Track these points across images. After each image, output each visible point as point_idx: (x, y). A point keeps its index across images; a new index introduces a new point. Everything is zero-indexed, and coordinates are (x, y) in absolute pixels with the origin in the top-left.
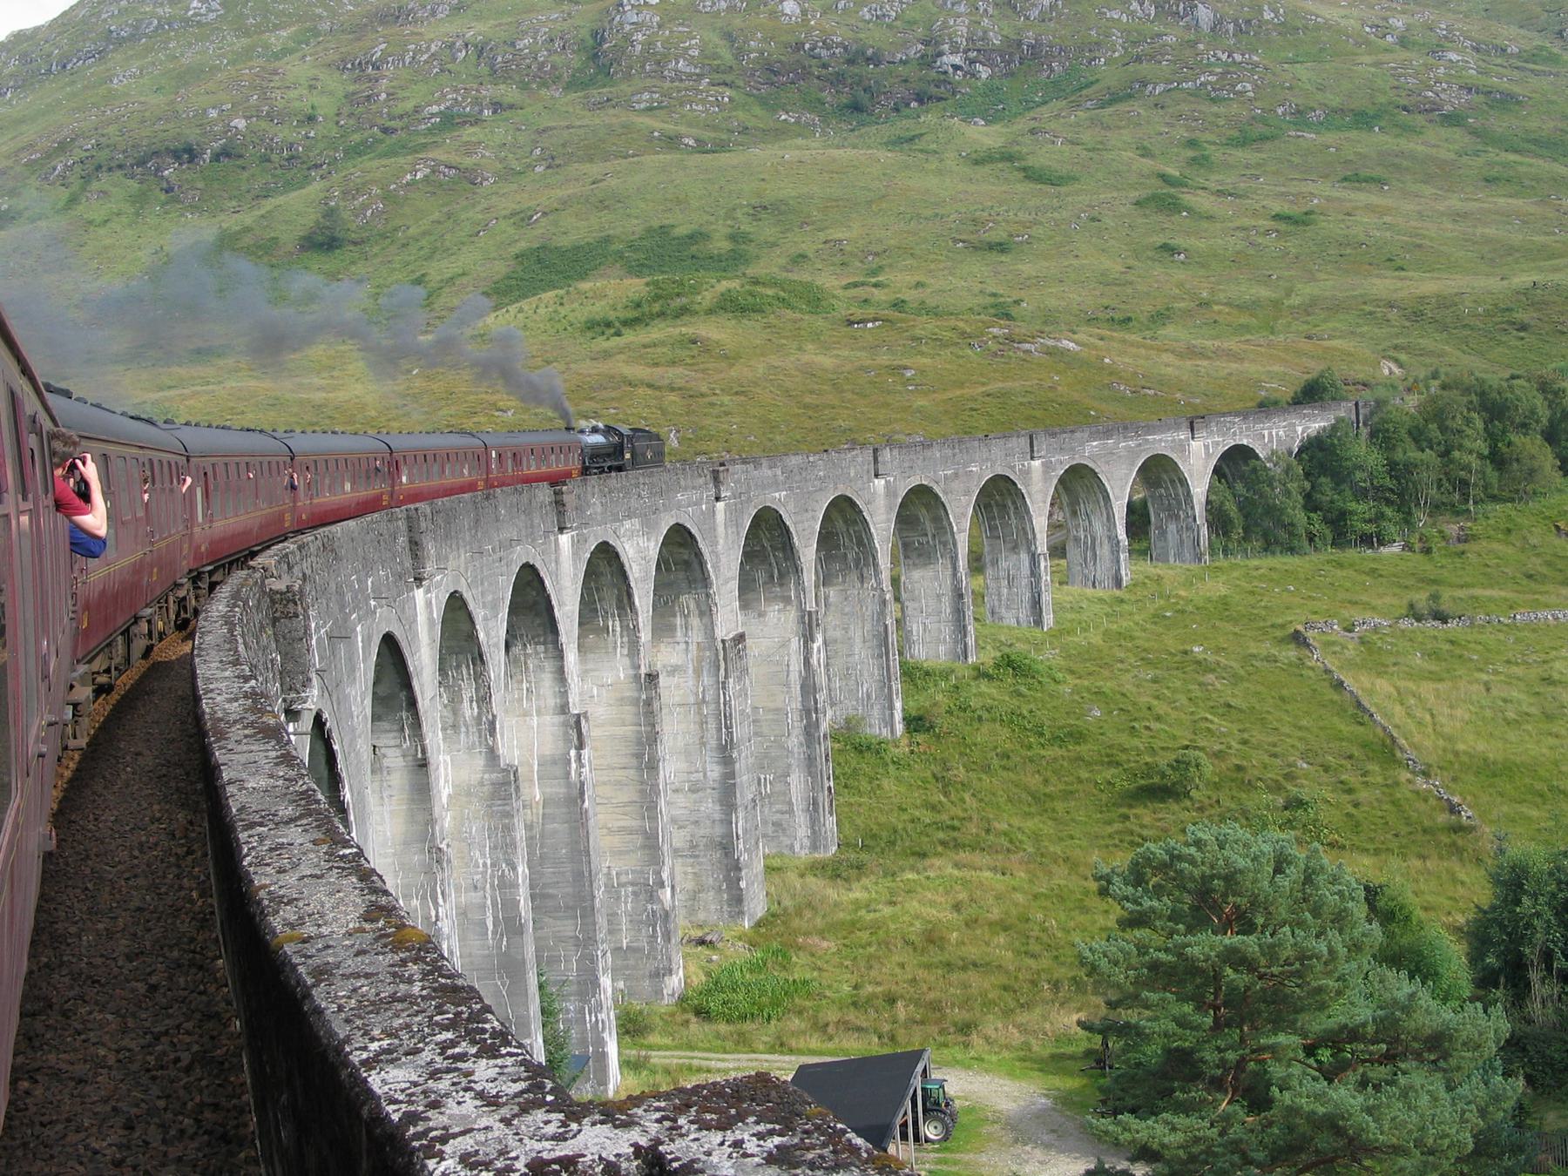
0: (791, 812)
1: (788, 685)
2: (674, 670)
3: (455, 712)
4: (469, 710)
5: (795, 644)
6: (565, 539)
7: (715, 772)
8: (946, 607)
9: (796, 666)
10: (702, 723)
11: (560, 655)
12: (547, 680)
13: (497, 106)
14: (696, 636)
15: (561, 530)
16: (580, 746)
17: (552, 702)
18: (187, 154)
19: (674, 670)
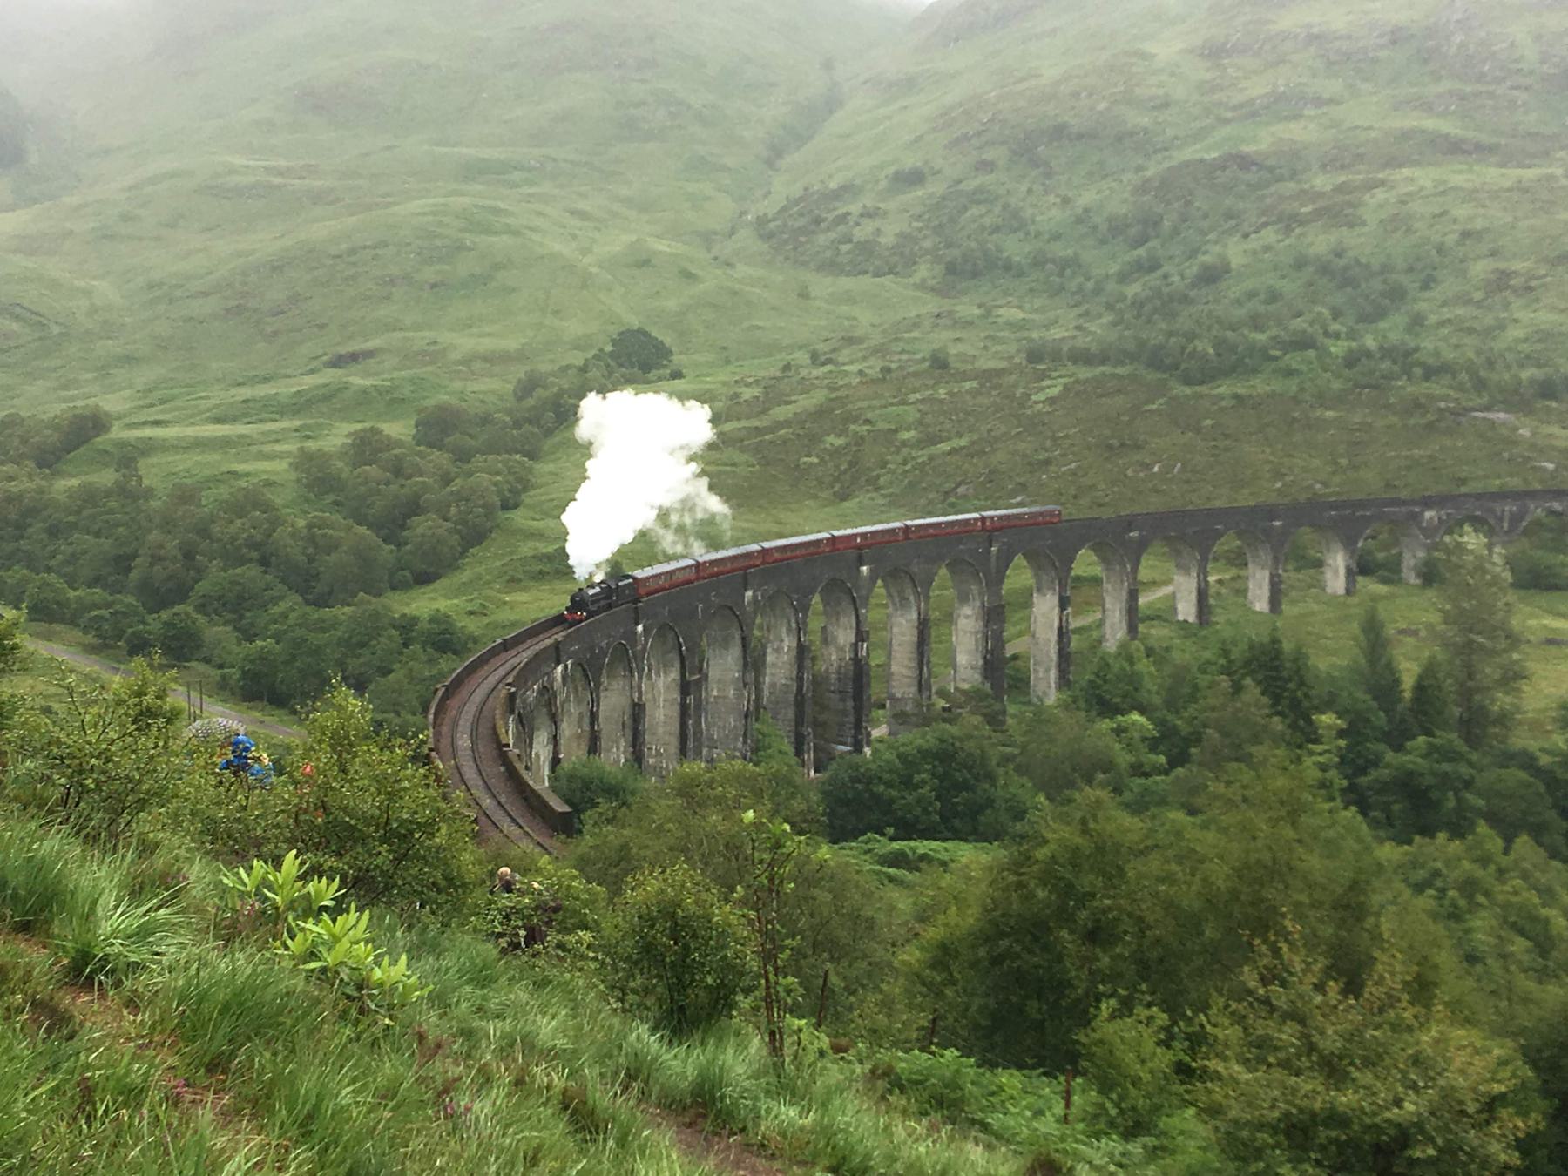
0: (1050, 687)
1: (1052, 626)
2: (967, 617)
3: (790, 625)
4: (794, 625)
5: (1057, 610)
6: (864, 568)
7: (981, 662)
8: (1194, 596)
9: (1056, 624)
10: (977, 640)
11: (857, 610)
12: (853, 617)
13: (1319, 102)
14: (978, 604)
15: (862, 565)
16: (863, 641)
17: (854, 625)
18: (1058, 132)
19: (967, 617)
